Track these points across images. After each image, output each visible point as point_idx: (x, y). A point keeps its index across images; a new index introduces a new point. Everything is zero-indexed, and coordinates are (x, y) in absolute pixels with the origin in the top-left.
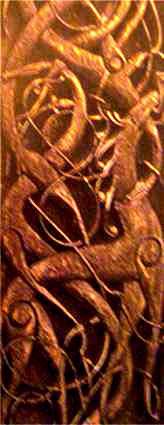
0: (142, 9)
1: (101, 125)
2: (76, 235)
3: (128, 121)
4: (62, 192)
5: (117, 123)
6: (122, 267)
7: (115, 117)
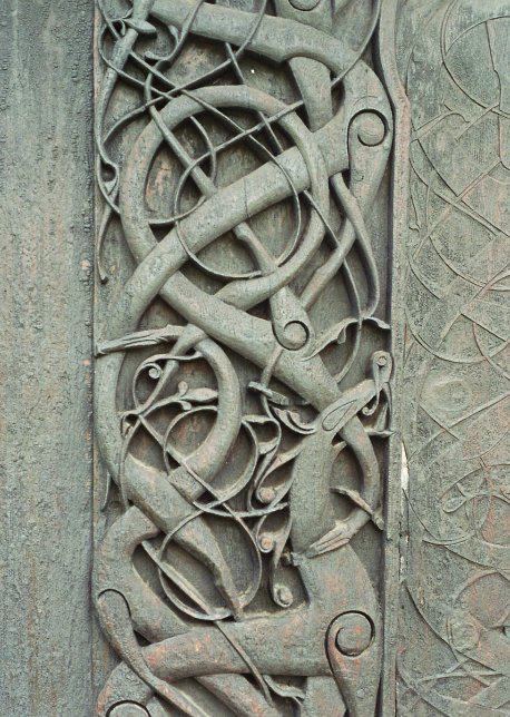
0: (344, 245)
1: (268, 430)
2: (220, 598)
3: (315, 426)
4: (198, 536)
5: (292, 427)
6: (301, 655)
7: (290, 417)
